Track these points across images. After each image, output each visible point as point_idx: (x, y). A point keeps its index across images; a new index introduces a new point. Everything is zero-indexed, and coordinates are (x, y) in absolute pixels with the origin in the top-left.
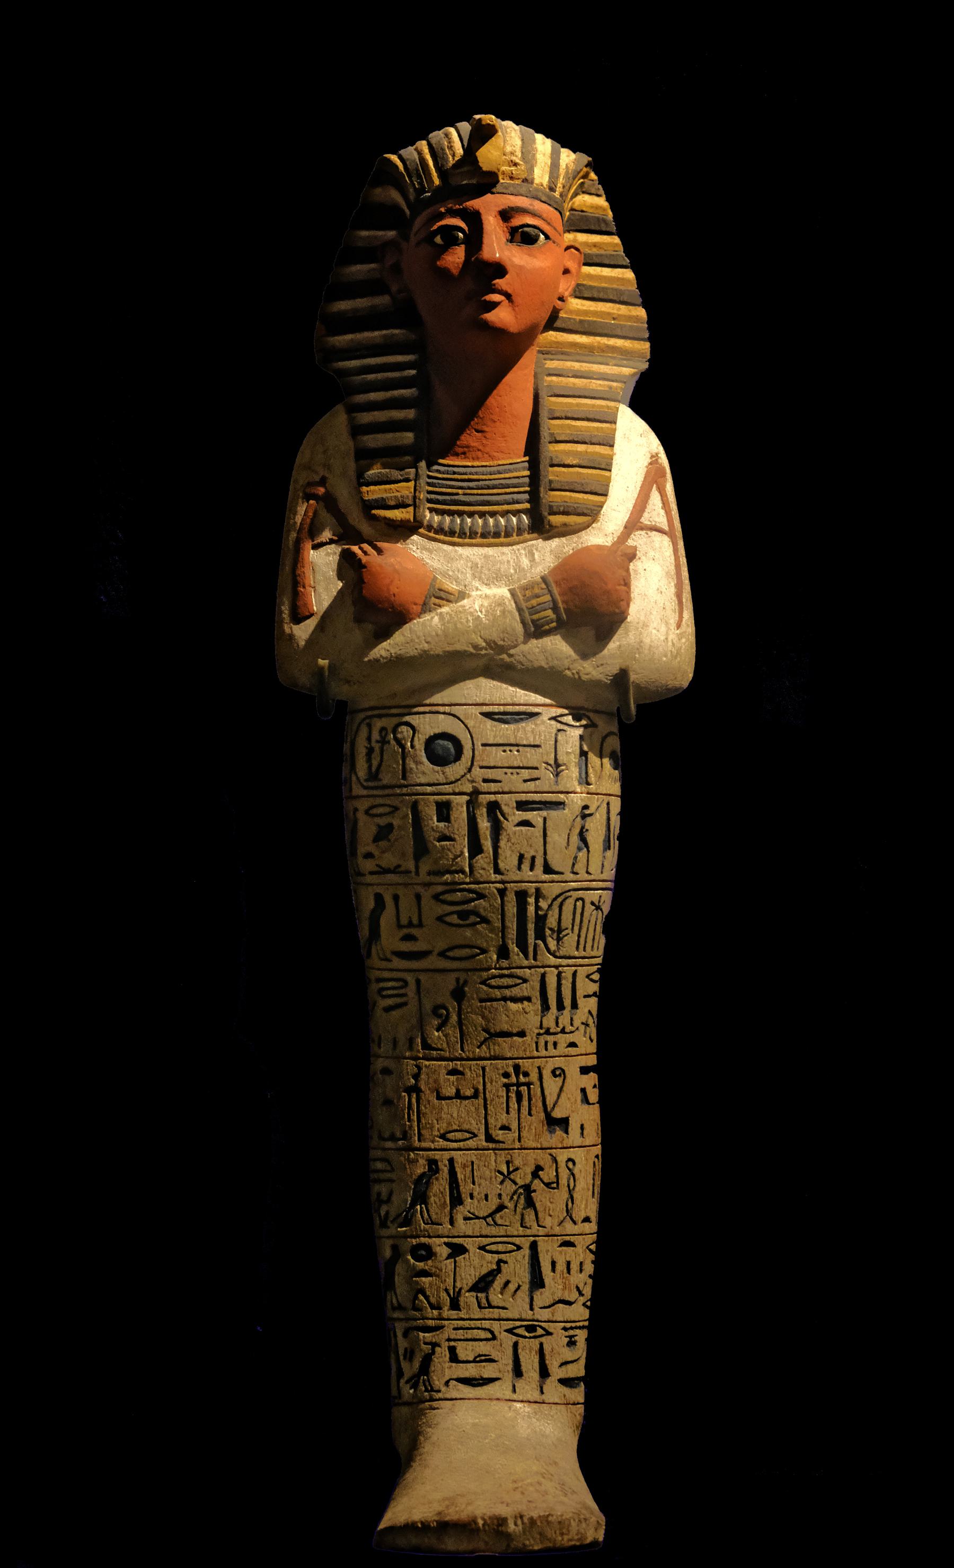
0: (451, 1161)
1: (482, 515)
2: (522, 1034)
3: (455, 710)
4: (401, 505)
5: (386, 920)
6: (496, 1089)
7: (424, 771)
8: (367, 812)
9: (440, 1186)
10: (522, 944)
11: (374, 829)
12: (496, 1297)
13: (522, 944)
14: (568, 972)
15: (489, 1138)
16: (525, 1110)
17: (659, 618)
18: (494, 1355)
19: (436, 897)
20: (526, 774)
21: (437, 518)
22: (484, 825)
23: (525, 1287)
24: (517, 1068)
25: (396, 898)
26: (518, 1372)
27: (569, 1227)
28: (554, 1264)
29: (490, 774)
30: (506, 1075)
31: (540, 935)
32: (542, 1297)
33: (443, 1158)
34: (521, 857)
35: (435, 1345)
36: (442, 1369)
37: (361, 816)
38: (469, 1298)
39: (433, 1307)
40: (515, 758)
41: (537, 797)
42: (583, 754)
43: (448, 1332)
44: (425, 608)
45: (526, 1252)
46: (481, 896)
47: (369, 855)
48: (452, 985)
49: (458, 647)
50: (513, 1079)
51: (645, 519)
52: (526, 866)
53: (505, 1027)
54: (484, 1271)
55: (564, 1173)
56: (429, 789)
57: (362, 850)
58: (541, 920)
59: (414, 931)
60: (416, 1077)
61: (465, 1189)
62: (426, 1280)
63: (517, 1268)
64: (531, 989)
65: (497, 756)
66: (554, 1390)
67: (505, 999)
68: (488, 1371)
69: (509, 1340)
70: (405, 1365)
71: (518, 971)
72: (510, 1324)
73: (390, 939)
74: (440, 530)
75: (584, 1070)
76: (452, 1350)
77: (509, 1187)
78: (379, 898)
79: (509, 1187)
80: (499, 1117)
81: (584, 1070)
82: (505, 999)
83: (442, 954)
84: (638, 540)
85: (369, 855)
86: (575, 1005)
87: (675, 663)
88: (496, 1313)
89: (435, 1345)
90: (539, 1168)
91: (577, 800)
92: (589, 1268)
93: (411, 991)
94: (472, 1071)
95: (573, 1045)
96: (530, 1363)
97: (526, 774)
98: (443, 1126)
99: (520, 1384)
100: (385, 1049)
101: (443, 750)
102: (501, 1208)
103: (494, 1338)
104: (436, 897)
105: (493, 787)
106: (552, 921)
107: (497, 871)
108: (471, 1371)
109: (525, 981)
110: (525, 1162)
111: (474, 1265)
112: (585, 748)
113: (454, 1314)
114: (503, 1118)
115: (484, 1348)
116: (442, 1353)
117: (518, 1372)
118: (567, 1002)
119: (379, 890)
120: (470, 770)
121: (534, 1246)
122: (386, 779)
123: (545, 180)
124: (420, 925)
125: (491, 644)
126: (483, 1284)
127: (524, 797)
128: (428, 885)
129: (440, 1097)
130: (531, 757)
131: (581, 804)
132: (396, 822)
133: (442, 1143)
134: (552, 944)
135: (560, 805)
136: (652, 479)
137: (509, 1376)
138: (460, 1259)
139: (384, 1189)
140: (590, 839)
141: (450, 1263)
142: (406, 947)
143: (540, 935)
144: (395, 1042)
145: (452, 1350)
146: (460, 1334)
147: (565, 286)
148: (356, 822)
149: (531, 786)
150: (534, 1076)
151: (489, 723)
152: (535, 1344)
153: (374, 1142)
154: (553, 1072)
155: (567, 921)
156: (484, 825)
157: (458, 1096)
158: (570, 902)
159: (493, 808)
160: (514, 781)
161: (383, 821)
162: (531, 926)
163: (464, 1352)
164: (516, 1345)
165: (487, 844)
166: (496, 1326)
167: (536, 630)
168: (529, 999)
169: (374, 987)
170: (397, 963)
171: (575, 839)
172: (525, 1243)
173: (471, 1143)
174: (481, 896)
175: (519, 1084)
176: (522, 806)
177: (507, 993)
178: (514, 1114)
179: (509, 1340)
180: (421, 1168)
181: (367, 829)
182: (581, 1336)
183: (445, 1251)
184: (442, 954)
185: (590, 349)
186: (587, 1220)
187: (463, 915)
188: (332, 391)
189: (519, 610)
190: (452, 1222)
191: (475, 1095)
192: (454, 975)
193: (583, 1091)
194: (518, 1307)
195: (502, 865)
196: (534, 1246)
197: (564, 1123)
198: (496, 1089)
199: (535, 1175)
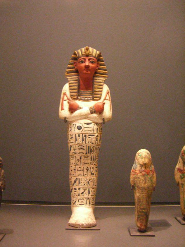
0: (79, 178)
1: (85, 97)
2: (88, 163)
3: (81, 123)
4: (75, 96)
5: (72, 148)
6: (85, 170)
7: (77, 130)
8: (70, 135)
9: (77, 182)
10: (89, 152)
11: (70, 137)
12: (84, 195)
13: (89, 152)
14: (94, 156)
15: (84, 176)
16: (88, 172)
17: (108, 112)
18: (84, 201)
19: (78, 146)
20: (90, 131)
21: (80, 98)
22: (84, 138)
23: (88, 194)
24: (88, 167)
25: (73, 146)
26: (86, 204)
27: (93, 186)
28: (91, 191)
29: (86, 131)
30: (86, 168)
31: (91, 151)
32: (90, 195)
33: (78, 178)
34: (89, 142)
35: (76, 200)
36: (77, 203)
37: (69, 135)
38: (81, 195)
39: (76, 195)
40: (89, 129)
41: (91, 134)
42: (97, 129)
43: (78, 199)
44: (78, 110)
45: (88, 190)
46: (84, 146)
47: (70, 140)
48: (80, 157)
49: (82, 115)
50: (87, 169)
51: (107, 98)
52: (89, 143)
53: (86, 162)
54: (83, 192)
55: (93, 180)
56: (77, 133)
57: (69, 140)
58: (91, 149)
59: (75, 150)
60: (75, 168)
61: (81, 181)
62: (75, 192)
63: (87, 191)
64: (90, 158)
65: (86, 129)
66: (91, 206)
67: (86, 159)
68: (83, 203)
69: (86, 200)
70: (73, 201)
71: (88, 156)
72: (86, 198)
73: (72, 151)
74: (80, 99)
75: (96, 167)
76: (78, 201)
77: (86, 182)
78: (71, 146)
79: (86, 182)
80: (85, 173)
81: (96, 167)
82: (86, 159)
83: (79, 153)
84: (105, 101)
85: (70, 140)
86: (95, 160)
87: (109, 117)
88: (84, 197)
89: (76, 200)
90: (90, 180)
91: (96, 135)
92: (96, 191)
93: (75, 157)
94: (82, 167)
95: (95, 164)
96: (88, 202)
97: (90, 131)
98: (78, 174)
99: (86, 205)
100: (72, 164)
101: (79, 128)
102: (85, 184)
103: (84, 199)
104: (78, 146)
105: (86, 133)
106: (93, 149)
107: (86, 143)
108: (81, 203)
109: (89, 157)
110: (88, 179)
111: (81, 191)
112: (98, 128)
113: (79, 196)
114: (86, 173)
115: (82, 201)
116: (77, 202)
117: (86, 204)
118: (94, 159)
119: (71, 145)
120: (83, 130)
121: (89, 189)
122: (72, 131)
123: (95, 55)
124: (76, 149)
125: (86, 115)
126: (83, 193)
127: (90, 134)
128: (77, 145)
129: (78, 170)
130: (91, 129)
131: (97, 135)
132: (73, 137)
133: (78, 176)
134: (92, 152)
135: (94, 135)
136: (108, 93)
137: (85, 204)
138: (80, 190)
139: (71, 181)
140: (98, 139)
141: (78, 191)
142: (74, 152)
143: (91, 151)
144: (73, 163)
145: (78, 201)
146: (80, 199)
147: (97, 68)
148: (68, 136)
149: (90, 133)
150: (90, 168)
151: (85, 125)
152: (89, 200)
153: (70, 175)
154: (92, 168)
155: (94, 150)
156: (84, 138)
157: (80, 170)
158: (95, 148)
159: (85, 136)
160: (88, 132)
161: (72, 136)
162: (90, 150)
163: (80, 201)
164: (86, 201)
165: (84, 140)
166: (84, 198)
167: (92, 113)
168: (89, 159)
169: (70, 156)
170: (73, 154)
171: (96, 140)
172: (88, 188)
173: (82, 176)
174: (84, 146)
175: (88, 169)
176: (89, 135)
177: (87, 158)
178: (87, 173)
179: (86, 200)
180: (75, 179)
181: (70, 137)
182: (94, 199)
183: (78, 189)
184: (79, 153)
185: (100, 76)
186: (96, 186)
187: (81, 149)
188: (67, 81)
189: (90, 110)
190: (79, 185)
191: (82, 171)
192: (80, 156)
193: (96, 170)
194: (87, 196)
195: (86, 143)
196: (89, 189)
197: (93, 174)
198: (85, 170)
199: (89, 180)
